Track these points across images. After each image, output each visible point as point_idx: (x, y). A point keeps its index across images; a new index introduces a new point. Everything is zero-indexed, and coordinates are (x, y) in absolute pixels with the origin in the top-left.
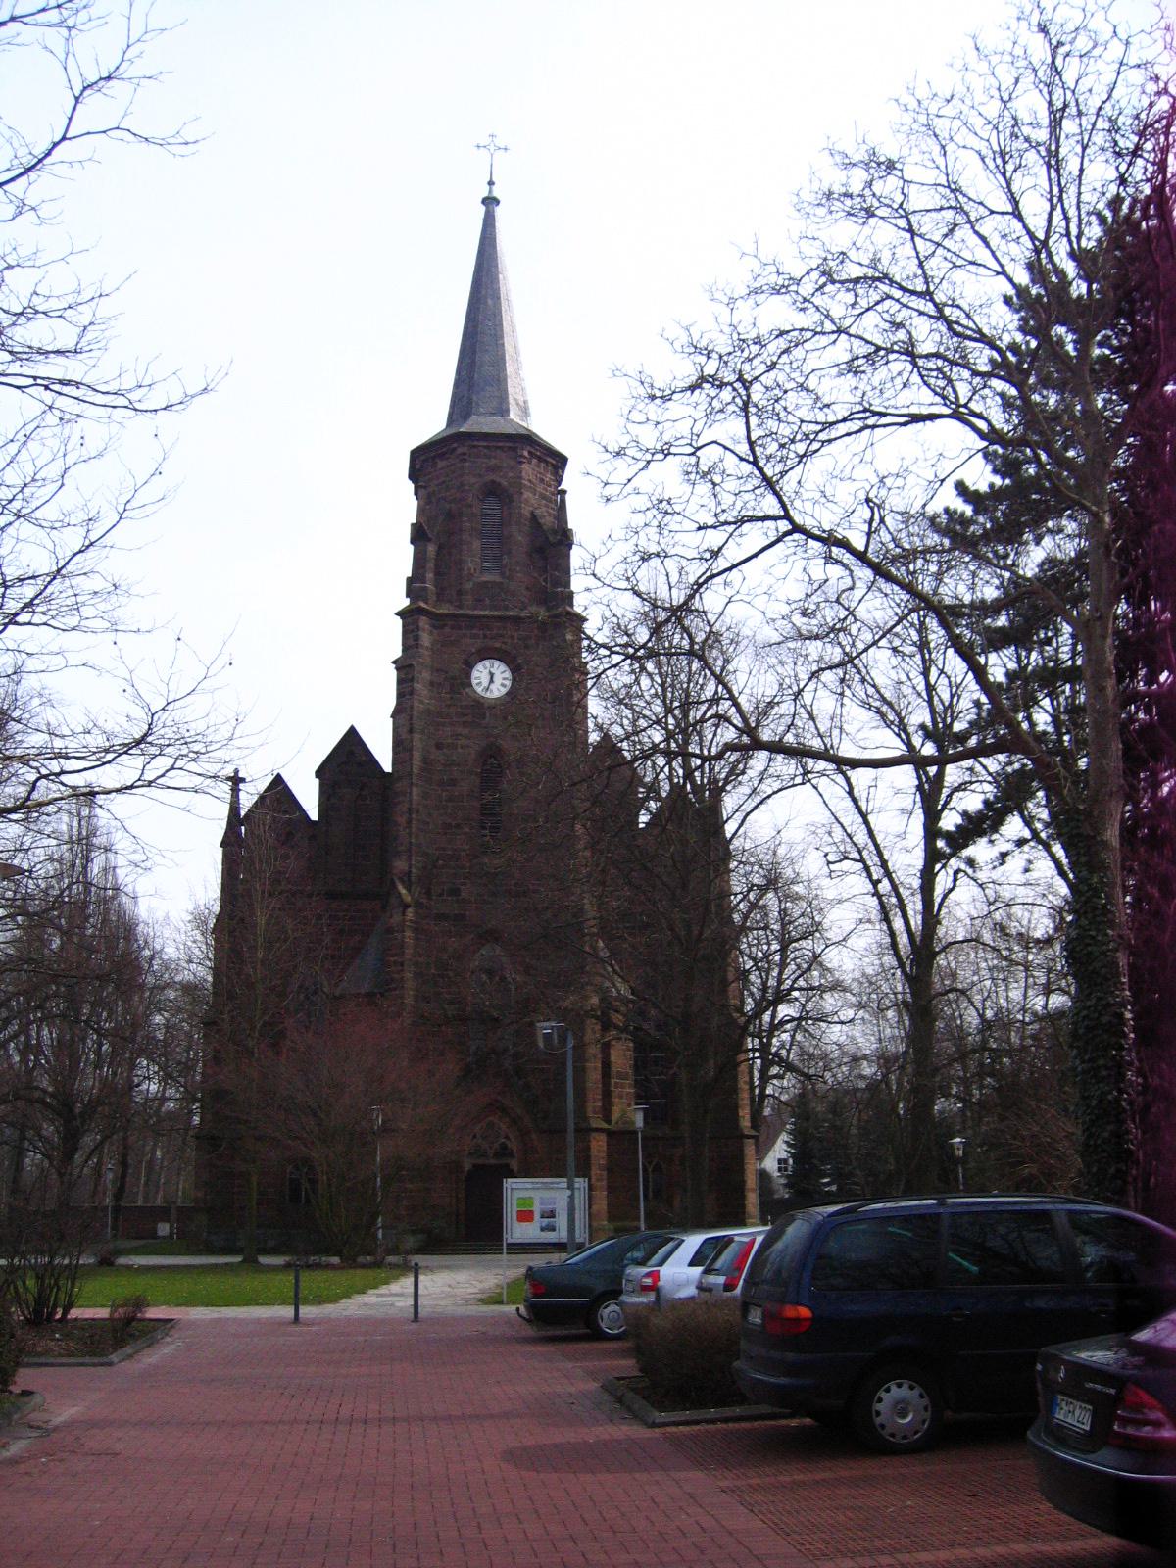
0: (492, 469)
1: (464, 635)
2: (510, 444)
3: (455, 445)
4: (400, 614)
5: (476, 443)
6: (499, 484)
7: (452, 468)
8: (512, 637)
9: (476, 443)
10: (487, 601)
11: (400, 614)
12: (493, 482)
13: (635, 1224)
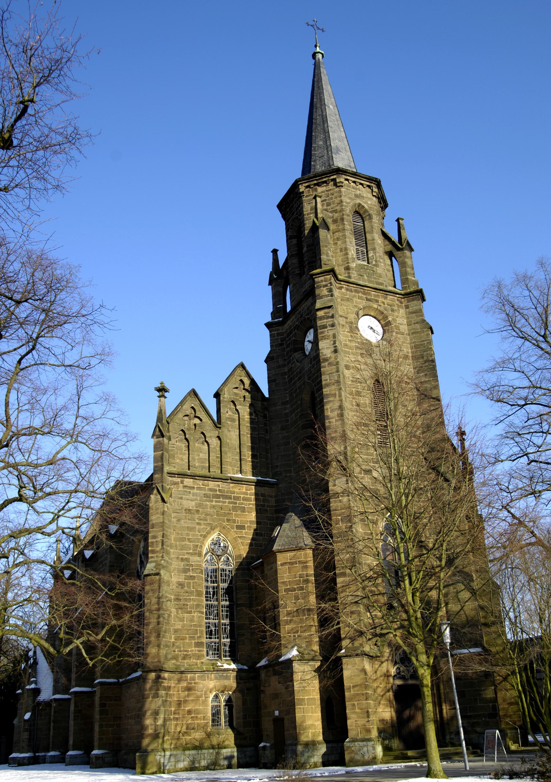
0: (357, 196)
1: (355, 296)
2: (368, 183)
3: (335, 177)
4: (268, 325)
5: (348, 178)
6: (363, 207)
7: (332, 192)
8: (384, 303)
9: (348, 178)
10: (366, 277)
11: (268, 325)
12: (360, 205)
13: (493, 755)
